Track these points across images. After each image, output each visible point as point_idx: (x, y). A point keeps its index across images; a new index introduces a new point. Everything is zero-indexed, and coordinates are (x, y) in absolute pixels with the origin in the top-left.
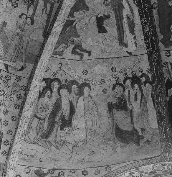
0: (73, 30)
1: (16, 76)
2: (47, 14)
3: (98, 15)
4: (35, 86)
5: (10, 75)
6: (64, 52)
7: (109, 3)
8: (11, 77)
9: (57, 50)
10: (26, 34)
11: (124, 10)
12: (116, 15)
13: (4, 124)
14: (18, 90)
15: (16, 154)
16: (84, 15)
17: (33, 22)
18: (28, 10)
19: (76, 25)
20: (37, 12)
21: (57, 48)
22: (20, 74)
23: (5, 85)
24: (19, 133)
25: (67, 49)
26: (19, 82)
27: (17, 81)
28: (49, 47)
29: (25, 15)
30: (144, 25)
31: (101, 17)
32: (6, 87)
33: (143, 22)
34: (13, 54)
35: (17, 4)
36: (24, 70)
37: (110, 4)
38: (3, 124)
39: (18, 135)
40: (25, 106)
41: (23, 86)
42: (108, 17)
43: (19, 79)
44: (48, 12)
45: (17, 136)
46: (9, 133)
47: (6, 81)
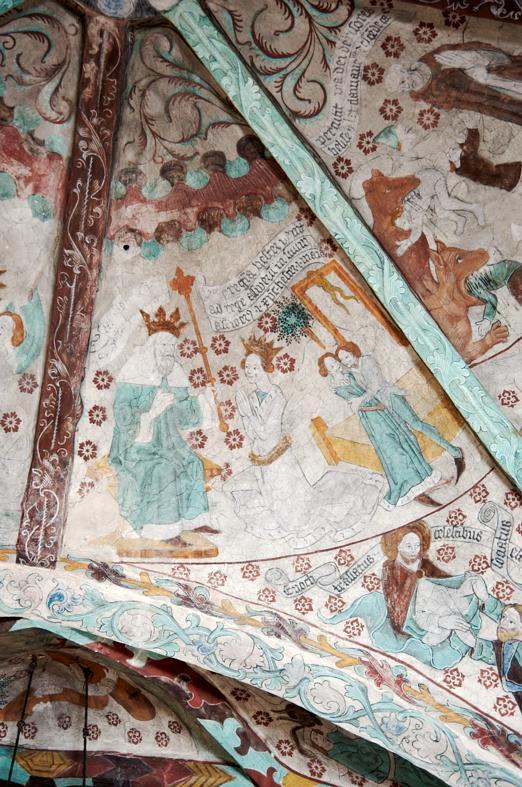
0: (447, 256)
2: (352, 297)
3: (451, 163)
5: (450, 508)
6: (503, 323)
7: (431, 111)
9: (476, 337)
10: (375, 386)
11: (469, 72)
12: (479, 107)
16: (424, 203)
17: (354, 350)
18: (318, 341)
19: (437, 242)
20: (332, 318)
21: (469, 333)
22: (469, 478)
23: (467, 540)
25: (498, 309)
26: (488, 498)
28: (429, 344)
29: (327, 355)
30: (514, 16)
31: (463, 159)
33: (502, 14)
34: (406, 458)
35: (286, 356)
36: (466, 461)
37: (436, 110)
41: (507, 494)
42: (474, 136)
43: (479, 492)
44: (348, 291)
47: (460, 529)
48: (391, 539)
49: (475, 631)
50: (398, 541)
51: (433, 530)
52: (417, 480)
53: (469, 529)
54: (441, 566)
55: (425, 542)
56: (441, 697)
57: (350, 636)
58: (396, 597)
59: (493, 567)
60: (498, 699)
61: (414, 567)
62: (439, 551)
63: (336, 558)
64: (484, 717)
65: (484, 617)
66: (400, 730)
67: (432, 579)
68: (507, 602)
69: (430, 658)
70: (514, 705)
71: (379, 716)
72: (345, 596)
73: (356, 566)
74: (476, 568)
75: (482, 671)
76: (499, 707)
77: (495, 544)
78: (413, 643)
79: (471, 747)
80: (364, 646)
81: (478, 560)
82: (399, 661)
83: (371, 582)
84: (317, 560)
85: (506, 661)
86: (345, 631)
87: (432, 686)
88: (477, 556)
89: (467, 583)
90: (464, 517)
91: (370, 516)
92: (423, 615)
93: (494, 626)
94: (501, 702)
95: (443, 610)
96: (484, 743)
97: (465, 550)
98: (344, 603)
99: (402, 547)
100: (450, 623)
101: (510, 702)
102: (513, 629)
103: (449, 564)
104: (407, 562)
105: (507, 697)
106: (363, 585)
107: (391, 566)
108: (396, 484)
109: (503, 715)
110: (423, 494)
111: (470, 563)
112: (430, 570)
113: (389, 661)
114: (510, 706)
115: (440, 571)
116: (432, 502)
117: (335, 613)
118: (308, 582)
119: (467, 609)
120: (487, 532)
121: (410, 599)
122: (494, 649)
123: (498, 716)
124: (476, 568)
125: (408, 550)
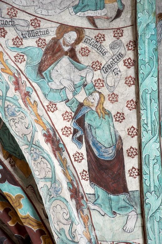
1: (112, 31)
4: (145, 25)
5: (101, 32)
8: (104, 35)
13: (118, 119)
14: (123, 52)
15: (152, 163)
23: (99, 51)
24: (145, 122)
26: (121, 38)
27: (118, 38)
32: (102, 54)
38: (116, 121)
39: (145, 126)
40: (140, 69)
41: (130, 41)
43: (118, 32)
45: (142, 129)
46: (130, 133)
47: (99, 44)
48: (63, 29)
49: (75, 94)
50: (67, 32)
51: (86, 37)
52: (94, 8)
53: (102, 47)
54: (79, 56)
55: (78, 41)
56: (41, 111)
57: (16, 61)
58: (49, 56)
59: (102, 71)
60: (66, 127)
61: (66, 49)
62: (82, 48)
63: (31, 20)
64: (55, 131)
65: (83, 90)
66: (13, 114)
67: (71, 59)
68: (97, 90)
69: (47, 93)
70: (71, 133)
71: (7, 103)
72: (24, 41)
73: (38, 31)
74: (94, 66)
75: (67, 112)
76: (64, 130)
77: (110, 61)
78: (44, 83)
79: (40, 138)
80: (20, 69)
81: (97, 63)
82: (32, 86)
83: (41, 43)
84: (20, 15)
85: (80, 114)
86: (15, 57)
87: (40, 105)
88: (98, 61)
89: (85, 71)
90: (104, 40)
91: (60, 11)
92: (56, 72)
93: (85, 96)
94: (66, 129)
95: (66, 76)
96: (47, 141)
97: (94, 55)
98: (22, 44)
99: (66, 36)
100: (66, 83)
101: (70, 131)
102: (92, 103)
103: (83, 57)
104: (64, 44)
105: (70, 128)
106: (36, 42)
107: (55, 41)
108: (83, 4)
109: (63, 134)
110: (92, 17)
111: (93, 63)
112: (72, 54)
113: (28, 85)
114: (69, 132)
115: (78, 60)
116: (94, 24)
117: (15, 46)
118: (10, 23)
119: (78, 82)
120: (110, 53)
121: (54, 62)
122: (78, 106)
123: (61, 133)
124: (94, 66)
125: (68, 39)
